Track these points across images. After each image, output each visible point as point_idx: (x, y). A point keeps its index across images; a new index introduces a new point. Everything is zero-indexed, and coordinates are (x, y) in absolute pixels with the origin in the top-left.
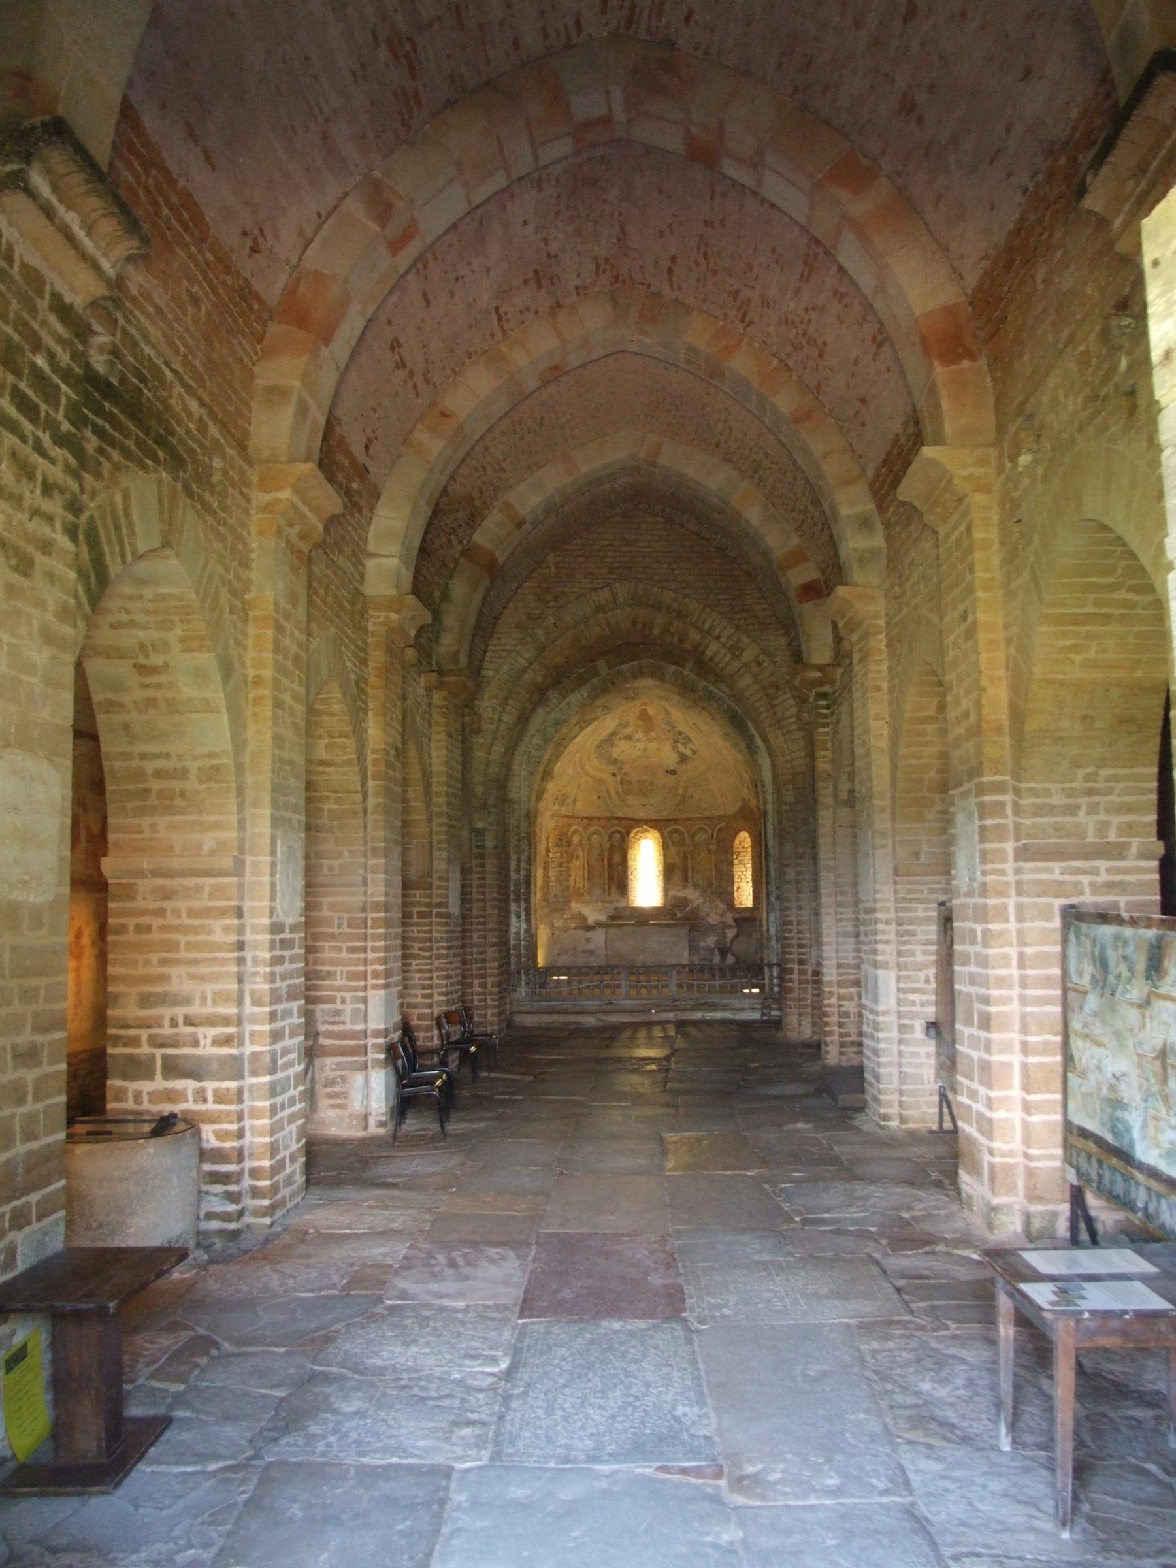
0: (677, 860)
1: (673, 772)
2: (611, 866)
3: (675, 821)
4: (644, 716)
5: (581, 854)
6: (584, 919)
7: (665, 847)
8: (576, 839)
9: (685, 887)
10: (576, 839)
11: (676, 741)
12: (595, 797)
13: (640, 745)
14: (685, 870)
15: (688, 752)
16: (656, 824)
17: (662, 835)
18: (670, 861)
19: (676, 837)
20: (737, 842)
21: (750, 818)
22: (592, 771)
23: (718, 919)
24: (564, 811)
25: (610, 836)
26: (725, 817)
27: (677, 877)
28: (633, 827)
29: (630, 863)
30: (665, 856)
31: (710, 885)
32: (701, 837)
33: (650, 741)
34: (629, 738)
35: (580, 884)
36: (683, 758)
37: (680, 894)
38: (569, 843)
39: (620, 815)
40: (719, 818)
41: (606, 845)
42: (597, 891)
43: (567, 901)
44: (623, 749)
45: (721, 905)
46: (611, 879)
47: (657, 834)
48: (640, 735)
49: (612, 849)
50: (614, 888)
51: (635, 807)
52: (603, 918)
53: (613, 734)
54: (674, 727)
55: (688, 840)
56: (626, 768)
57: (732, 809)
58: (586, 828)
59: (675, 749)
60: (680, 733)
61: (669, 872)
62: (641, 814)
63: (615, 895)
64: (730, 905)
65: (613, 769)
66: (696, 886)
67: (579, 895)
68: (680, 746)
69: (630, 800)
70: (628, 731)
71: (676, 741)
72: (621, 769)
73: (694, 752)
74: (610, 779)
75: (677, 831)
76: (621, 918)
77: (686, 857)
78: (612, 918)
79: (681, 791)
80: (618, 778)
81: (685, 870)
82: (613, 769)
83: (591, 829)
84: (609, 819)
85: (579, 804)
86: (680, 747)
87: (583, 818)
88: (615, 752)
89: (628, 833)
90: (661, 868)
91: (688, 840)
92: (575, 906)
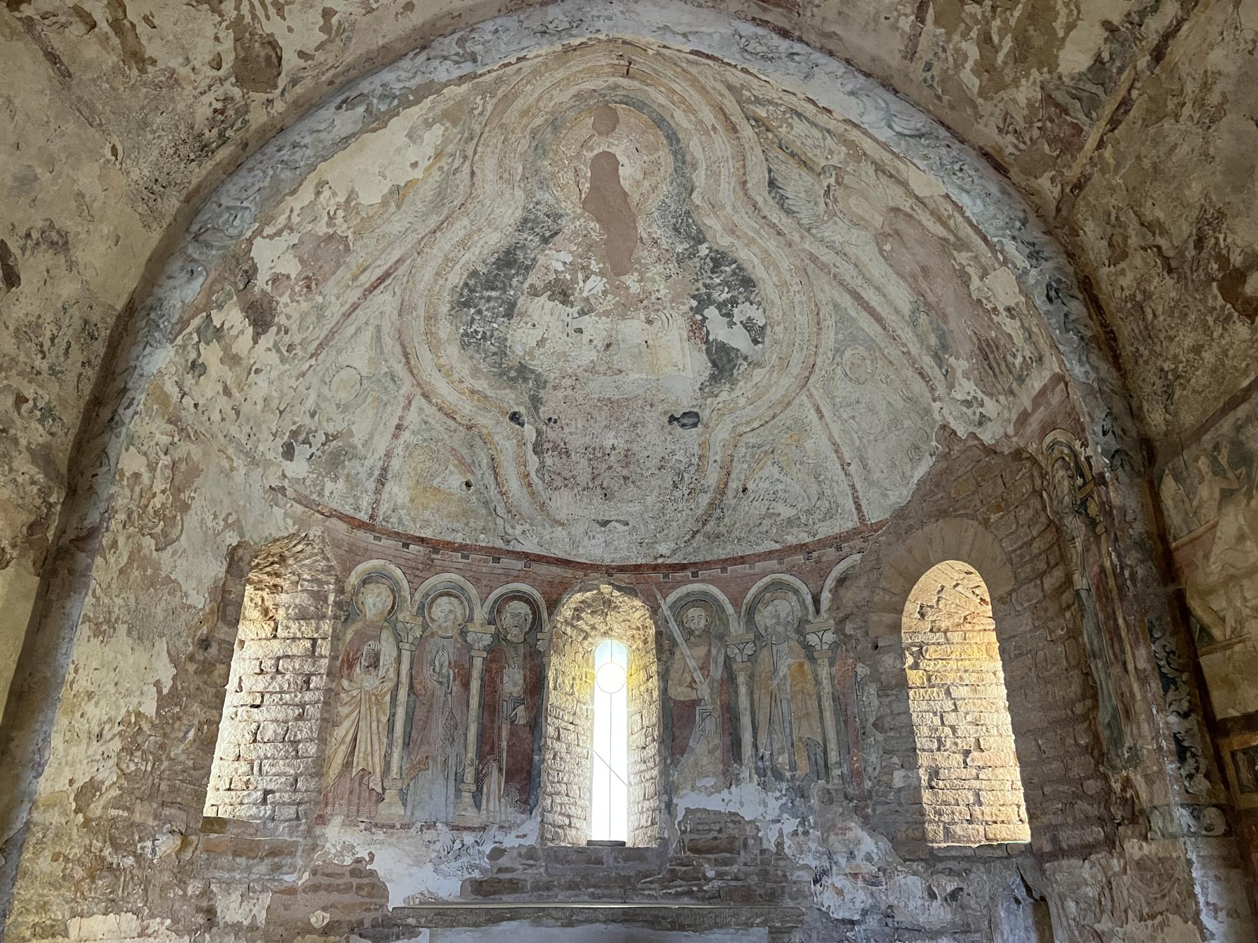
0: (704, 691)
1: (690, 419)
2: (490, 707)
3: (695, 568)
4: (606, 198)
5: (387, 649)
6: (377, 889)
7: (664, 647)
8: (374, 601)
9: (730, 779)
10: (374, 601)
11: (704, 302)
12: (455, 481)
13: (595, 326)
14: (730, 716)
15: (738, 340)
16: (640, 578)
17: (654, 610)
18: (680, 693)
19: (697, 618)
20: (911, 608)
21: (968, 495)
22: (443, 389)
23: (861, 898)
24: (334, 492)
25: (498, 608)
26: (864, 531)
27: (704, 743)
28: (565, 587)
29: (554, 698)
30: (664, 676)
31: (823, 770)
32: (784, 607)
33: (624, 310)
34: (561, 292)
35: (370, 756)
36: (723, 362)
37: (714, 803)
38: (347, 611)
39: (530, 547)
40: (837, 542)
41: (481, 636)
42: (436, 795)
43: (313, 815)
44: (539, 329)
45: (867, 843)
46: (487, 748)
47: (634, 611)
48: (595, 285)
49: (495, 655)
50: (495, 782)
51: (575, 527)
52: (449, 888)
53: (509, 261)
54: (699, 239)
55: (736, 628)
56: (552, 403)
57: (891, 489)
58: (417, 572)
59: (697, 328)
60: (718, 260)
61: (673, 727)
62: (593, 550)
63: (497, 804)
64: (912, 846)
65: (512, 399)
66: (768, 774)
67: (362, 798)
68: (711, 312)
69: (563, 503)
70: (556, 260)
71: (704, 302)
72: (536, 402)
73: (756, 333)
74: (505, 439)
75: (703, 600)
76: (514, 886)
77: (730, 678)
78: (480, 888)
79: (713, 477)
80: (529, 431)
81: (730, 716)
82: (512, 399)
83: (434, 580)
84: (495, 554)
85: (397, 492)
86: (719, 329)
87: (407, 541)
88: (521, 338)
89: (553, 604)
90: (652, 716)
91: (736, 628)
92: (340, 840)
